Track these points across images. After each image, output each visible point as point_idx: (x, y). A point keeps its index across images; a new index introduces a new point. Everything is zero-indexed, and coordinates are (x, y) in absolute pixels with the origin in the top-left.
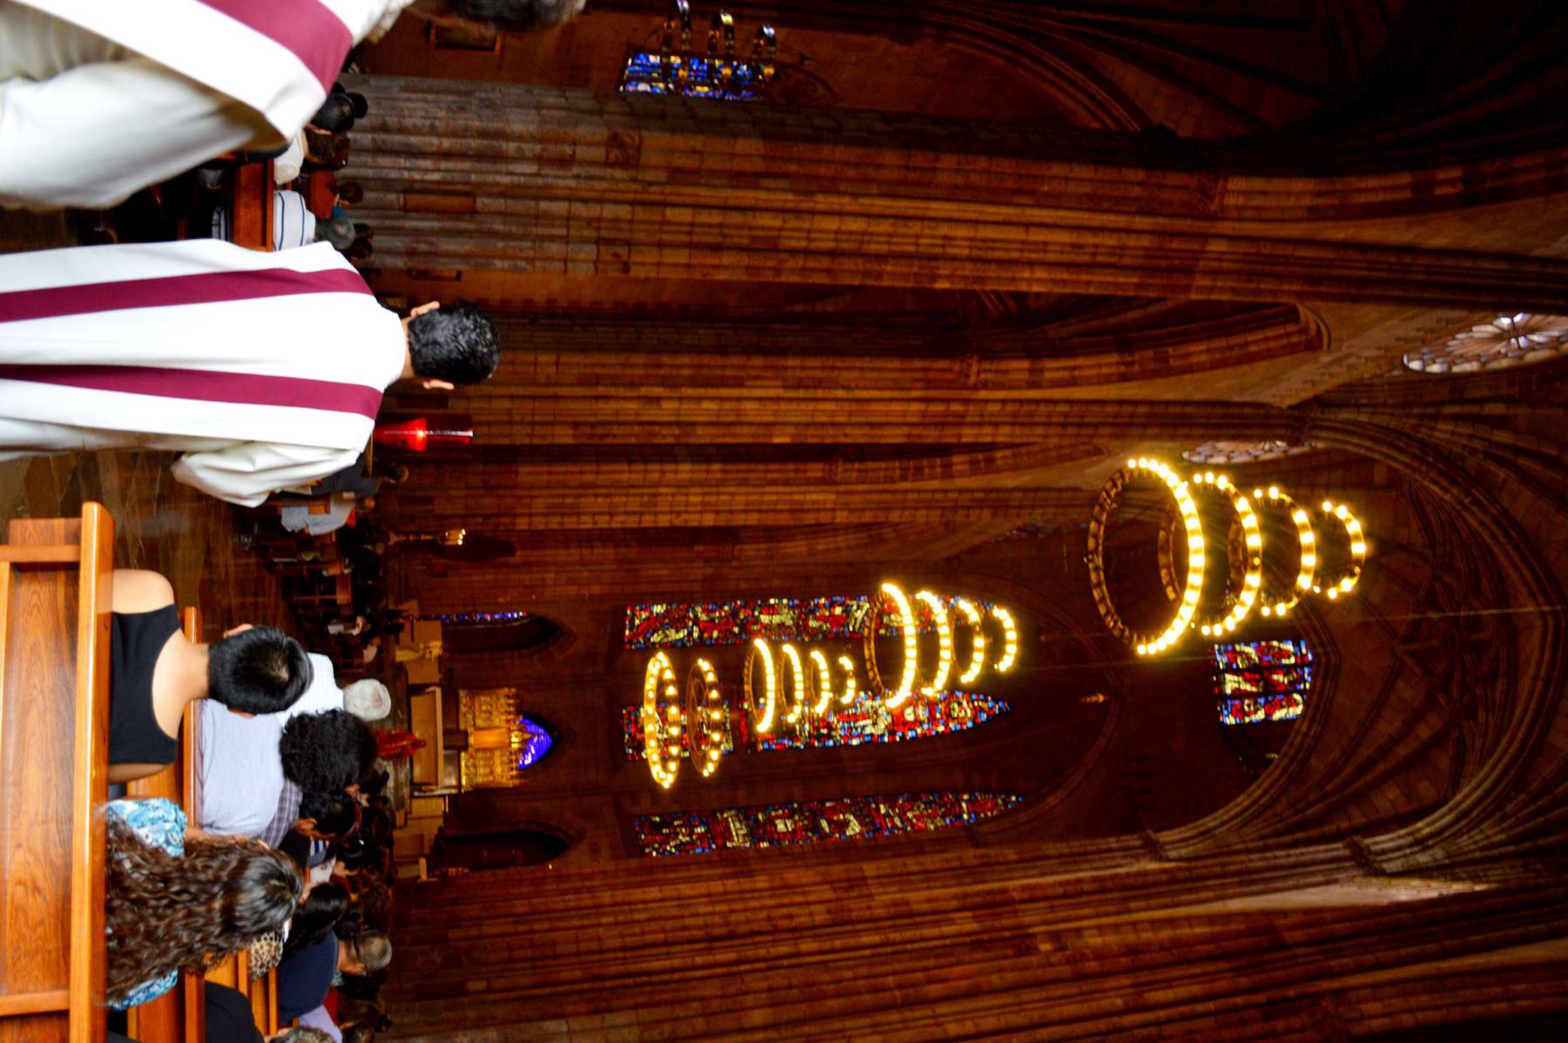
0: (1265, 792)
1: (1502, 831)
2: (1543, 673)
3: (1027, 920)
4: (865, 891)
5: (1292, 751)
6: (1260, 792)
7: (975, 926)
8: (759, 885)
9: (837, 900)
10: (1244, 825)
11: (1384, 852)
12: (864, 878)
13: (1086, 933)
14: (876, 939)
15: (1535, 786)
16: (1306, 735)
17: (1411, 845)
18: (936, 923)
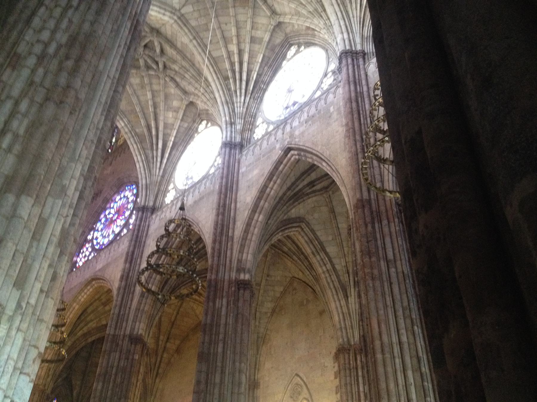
0: (140, 155)
1: (241, 96)
2: (191, 37)
3: (227, 277)
4: (121, 337)
5: (130, 135)
6: (139, 157)
7: (225, 301)
8: (99, 387)
9: (121, 352)
10: (150, 171)
11: (231, 137)
12: (114, 336)
13: (240, 258)
14: (221, 345)
15: (230, 74)
16: (126, 125)
17: (232, 127)
18: (219, 316)
